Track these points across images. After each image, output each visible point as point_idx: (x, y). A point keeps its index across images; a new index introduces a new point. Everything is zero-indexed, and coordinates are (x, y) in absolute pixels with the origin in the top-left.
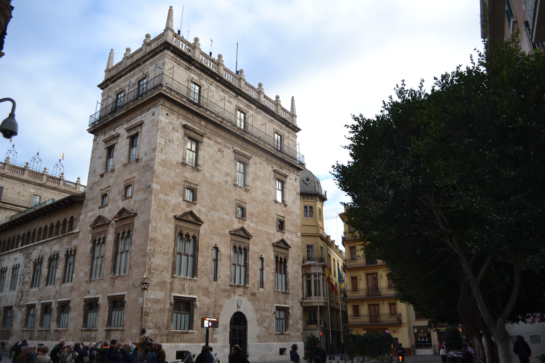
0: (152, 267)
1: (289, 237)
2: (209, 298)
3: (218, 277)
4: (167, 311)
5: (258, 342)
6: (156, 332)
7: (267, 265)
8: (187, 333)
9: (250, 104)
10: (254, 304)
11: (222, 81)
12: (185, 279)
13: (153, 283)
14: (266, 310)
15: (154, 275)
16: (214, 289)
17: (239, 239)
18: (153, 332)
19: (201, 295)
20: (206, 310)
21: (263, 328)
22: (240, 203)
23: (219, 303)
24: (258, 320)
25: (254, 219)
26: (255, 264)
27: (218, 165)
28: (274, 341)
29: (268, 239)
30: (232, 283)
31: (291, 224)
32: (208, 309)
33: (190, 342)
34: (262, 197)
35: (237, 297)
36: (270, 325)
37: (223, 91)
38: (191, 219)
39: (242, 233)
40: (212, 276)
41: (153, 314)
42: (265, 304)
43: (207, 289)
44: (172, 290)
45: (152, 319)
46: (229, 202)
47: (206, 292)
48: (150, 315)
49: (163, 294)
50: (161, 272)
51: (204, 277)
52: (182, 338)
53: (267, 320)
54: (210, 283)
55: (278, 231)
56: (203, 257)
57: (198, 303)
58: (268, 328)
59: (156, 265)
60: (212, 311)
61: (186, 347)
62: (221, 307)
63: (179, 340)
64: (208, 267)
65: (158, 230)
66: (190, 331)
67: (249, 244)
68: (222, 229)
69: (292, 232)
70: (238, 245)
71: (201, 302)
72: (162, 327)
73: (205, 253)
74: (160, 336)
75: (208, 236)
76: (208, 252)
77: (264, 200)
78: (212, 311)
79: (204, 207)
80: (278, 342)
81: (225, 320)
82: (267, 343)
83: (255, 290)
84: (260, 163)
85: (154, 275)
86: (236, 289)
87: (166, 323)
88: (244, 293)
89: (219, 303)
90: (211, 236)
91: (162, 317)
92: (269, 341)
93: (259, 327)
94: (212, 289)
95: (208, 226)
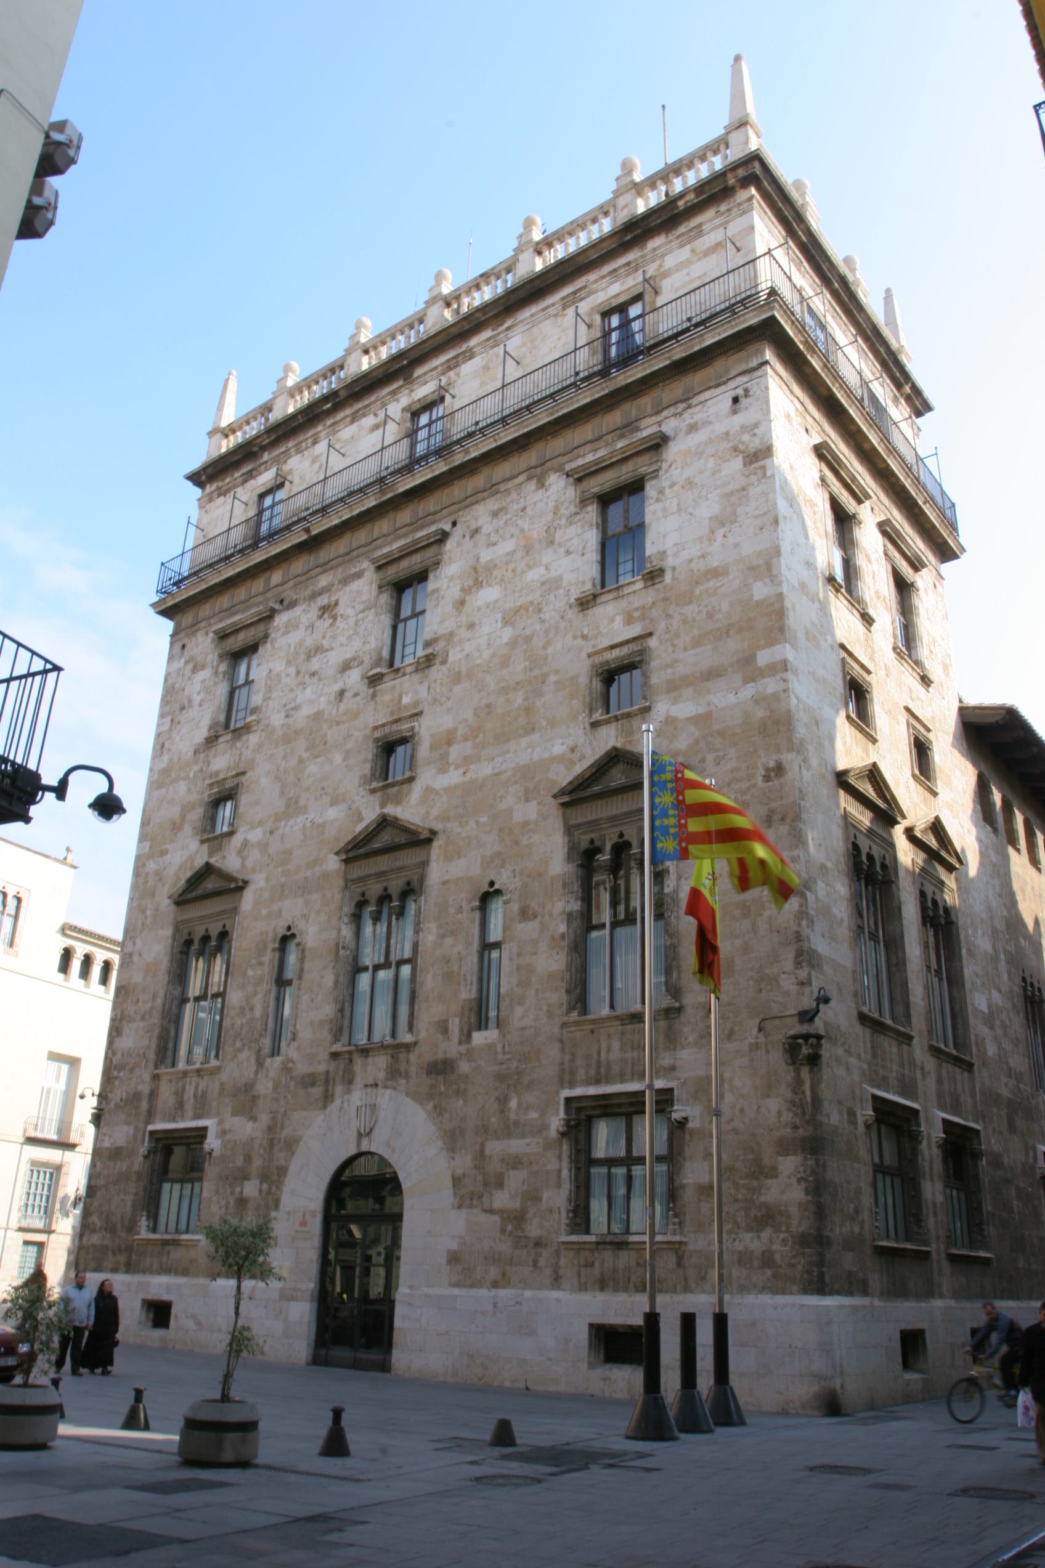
0: (114, 1062)
1: (684, 709)
2: (253, 1118)
3: (286, 1035)
4: (134, 1178)
5: (457, 1285)
6: (106, 1242)
7: (525, 914)
8: (176, 1243)
9: (464, 348)
10: (439, 1111)
11: (343, 394)
12: (185, 1073)
13: (112, 1105)
14: (509, 1129)
15: (117, 1083)
16: (270, 1085)
17: (382, 863)
18: (99, 1242)
19: (227, 1115)
20: (240, 1161)
21: (484, 1218)
22: (395, 728)
23: (286, 1132)
24: (457, 1181)
25: (455, 752)
26: (453, 933)
27: (315, 664)
28: (556, 1281)
29: (528, 796)
30: (337, 1047)
31: (697, 643)
32: (248, 1158)
33: (185, 1272)
34: (507, 633)
35: (357, 1097)
36: (532, 1197)
37: (354, 418)
38: (210, 884)
39: (385, 839)
40: (267, 1042)
41: (103, 1190)
42: (503, 1101)
43: (249, 1087)
44: (150, 1116)
45: (101, 1206)
46: (347, 755)
47: (245, 1100)
48: (98, 1194)
49: (131, 1130)
50: (132, 1070)
51: (240, 1050)
52: (165, 1259)
53: (516, 1179)
54: (260, 1064)
55: (595, 725)
56: (243, 987)
57: (212, 1142)
58: (517, 1218)
59: (123, 1055)
60: (257, 1163)
61: (168, 1288)
62: (291, 1145)
63: (155, 1266)
64: (258, 1013)
65: (136, 958)
66: (184, 1237)
67: (425, 864)
68: (316, 862)
69: (712, 674)
70: (374, 890)
71: (228, 1137)
72: (119, 1226)
73: (250, 973)
74: (114, 1254)
75: (264, 912)
76: (261, 964)
77: (513, 643)
78: (257, 1163)
79: (260, 824)
80: (583, 1287)
81: (304, 1193)
82: (502, 1292)
83: (451, 1048)
84: (495, 514)
85: (117, 1083)
86: (358, 1062)
87: (129, 1214)
88: (393, 1073)
89: (286, 1132)
90: (275, 907)
91: (122, 1196)
92: (525, 1284)
93: (463, 1214)
94: (264, 1087)
95: (267, 880)
